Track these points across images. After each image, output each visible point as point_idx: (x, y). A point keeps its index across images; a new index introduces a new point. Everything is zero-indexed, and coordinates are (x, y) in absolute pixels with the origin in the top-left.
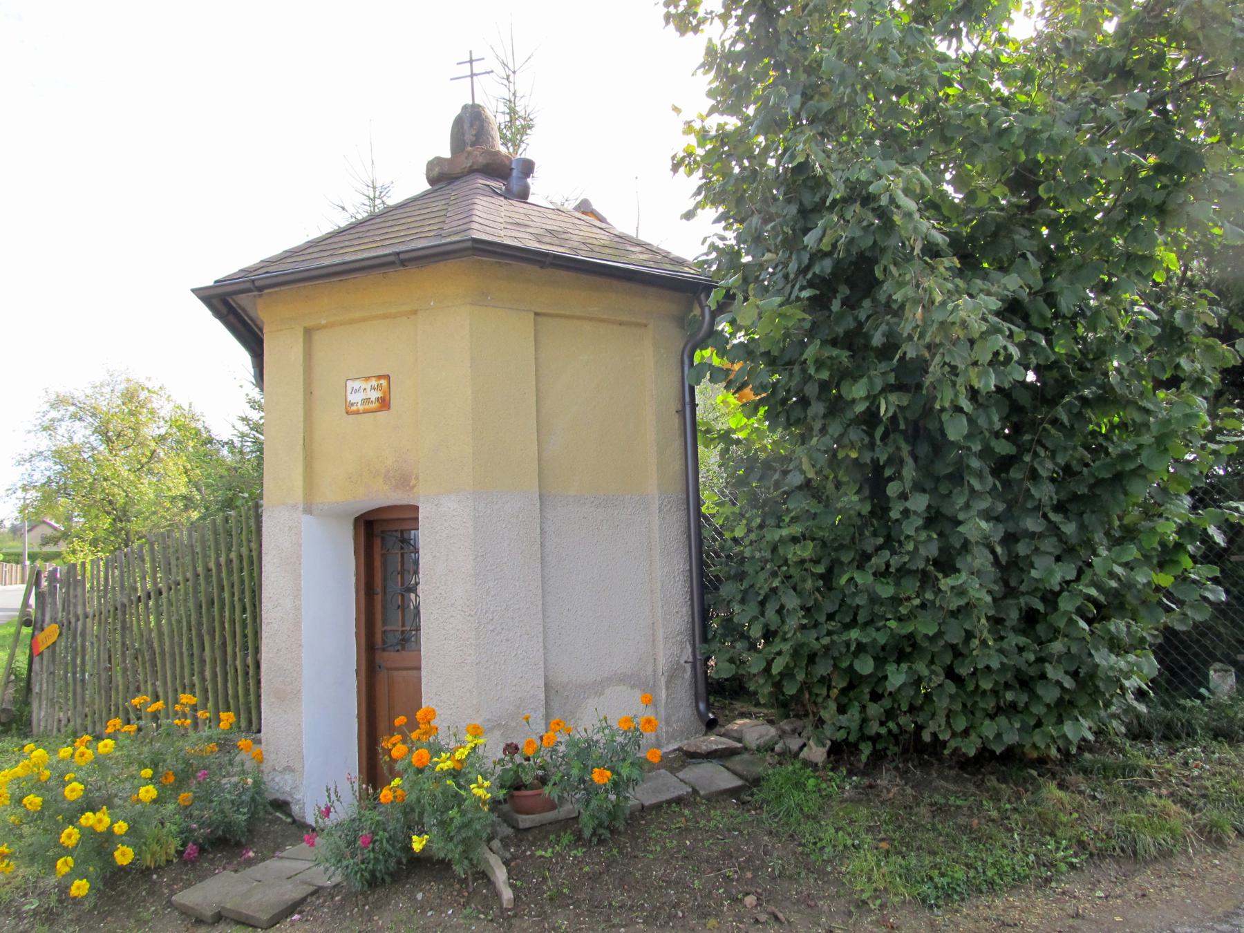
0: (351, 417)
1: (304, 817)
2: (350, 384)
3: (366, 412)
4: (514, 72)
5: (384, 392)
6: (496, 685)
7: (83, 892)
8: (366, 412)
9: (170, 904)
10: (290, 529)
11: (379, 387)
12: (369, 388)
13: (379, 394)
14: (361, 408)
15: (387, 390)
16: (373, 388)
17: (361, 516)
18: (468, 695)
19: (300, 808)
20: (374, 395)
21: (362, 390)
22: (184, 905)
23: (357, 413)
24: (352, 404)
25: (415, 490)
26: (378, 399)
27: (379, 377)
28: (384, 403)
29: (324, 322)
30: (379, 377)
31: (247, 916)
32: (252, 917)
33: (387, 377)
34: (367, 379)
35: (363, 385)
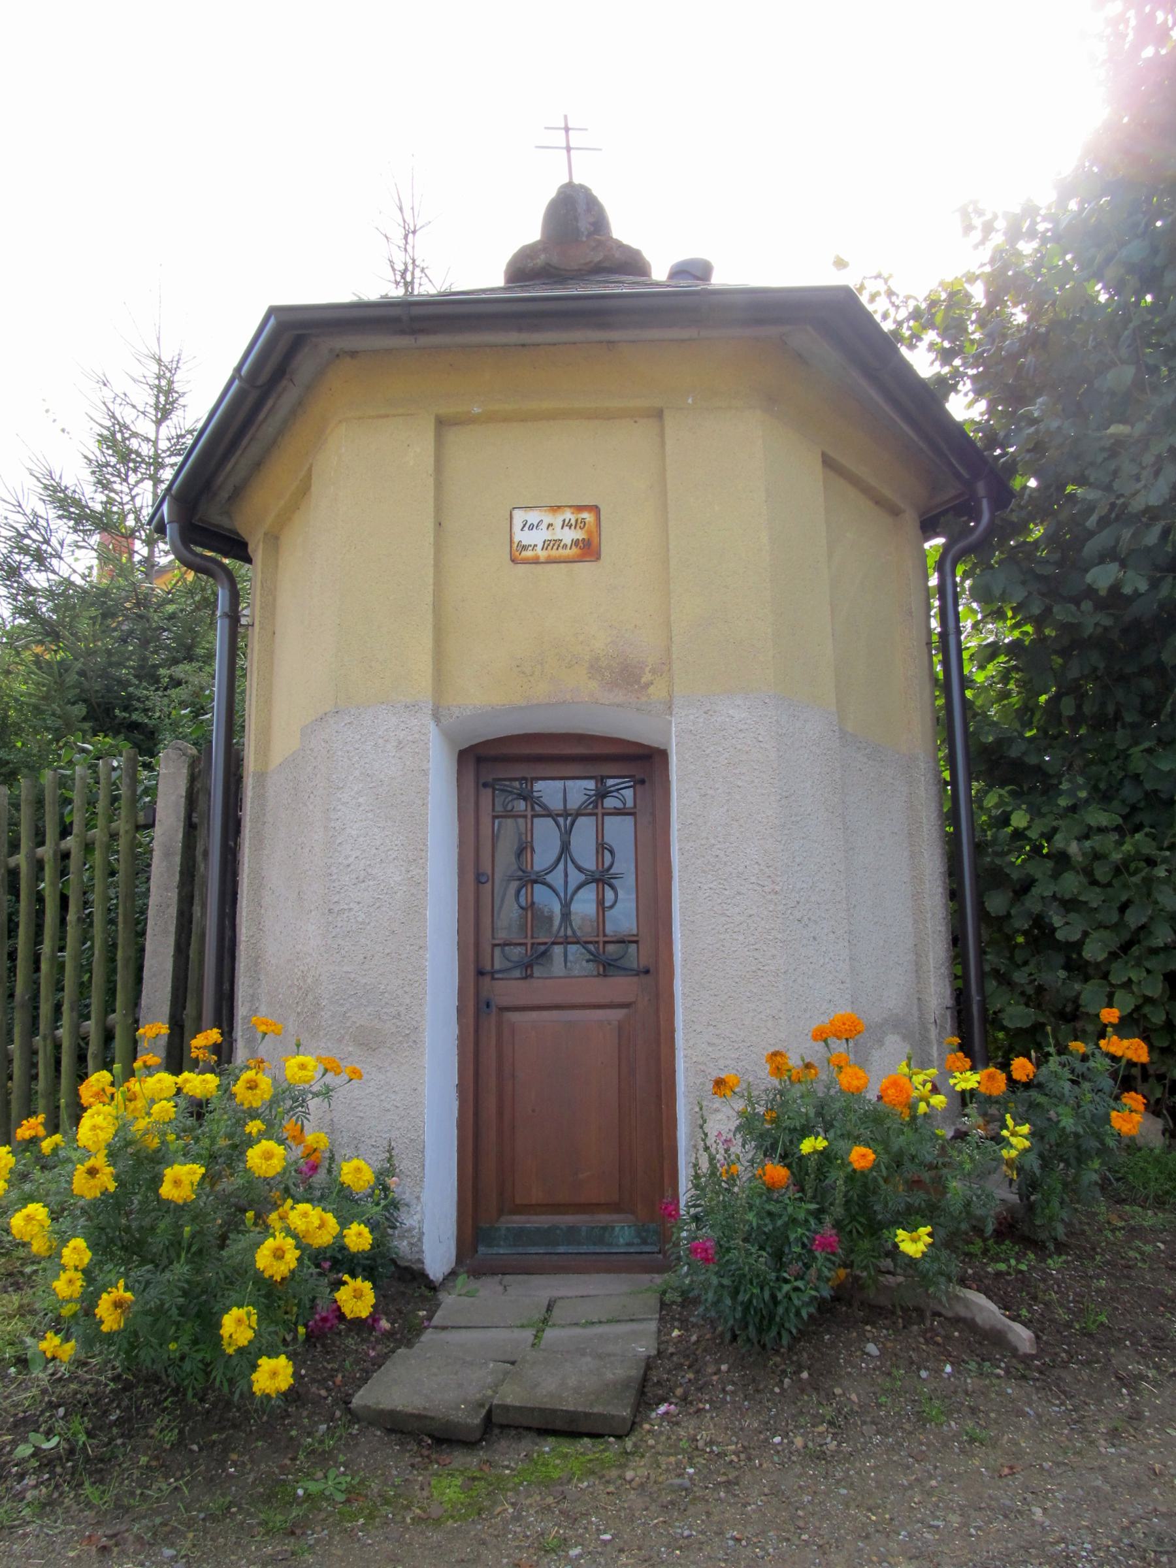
0: (522, 569)
1: (421, 1261)
2: (519, 517)
3: (550, 561)
4: (414, 232)
5: (589, 533)
6: (805, 1010)
7: (284, 1381)
8: (550, 561)
9: (354, 1416)
10: (400, 745)
11: (580, 524)
12: (558, 523)
13: (579, 535)
14: (543, 555)
15: (594, 529)
16: (566, 524)
17: (472, 748)
18: (770, 1024)
19: (411, 1245)
20: (569, 536)
21: (544, 526)
22: (392, 1414)
23: (536, 561)
24: (525, 548)
25: (651, 689)
26: (576, 543)
27: (580, 508)
28: (589, 550)
29: (477, 410)
30: (580, 508)
31: (572, 1416)
32: (587, 1415)
33: (595, 509)
34: (555, 509)
35: (547, 518)
